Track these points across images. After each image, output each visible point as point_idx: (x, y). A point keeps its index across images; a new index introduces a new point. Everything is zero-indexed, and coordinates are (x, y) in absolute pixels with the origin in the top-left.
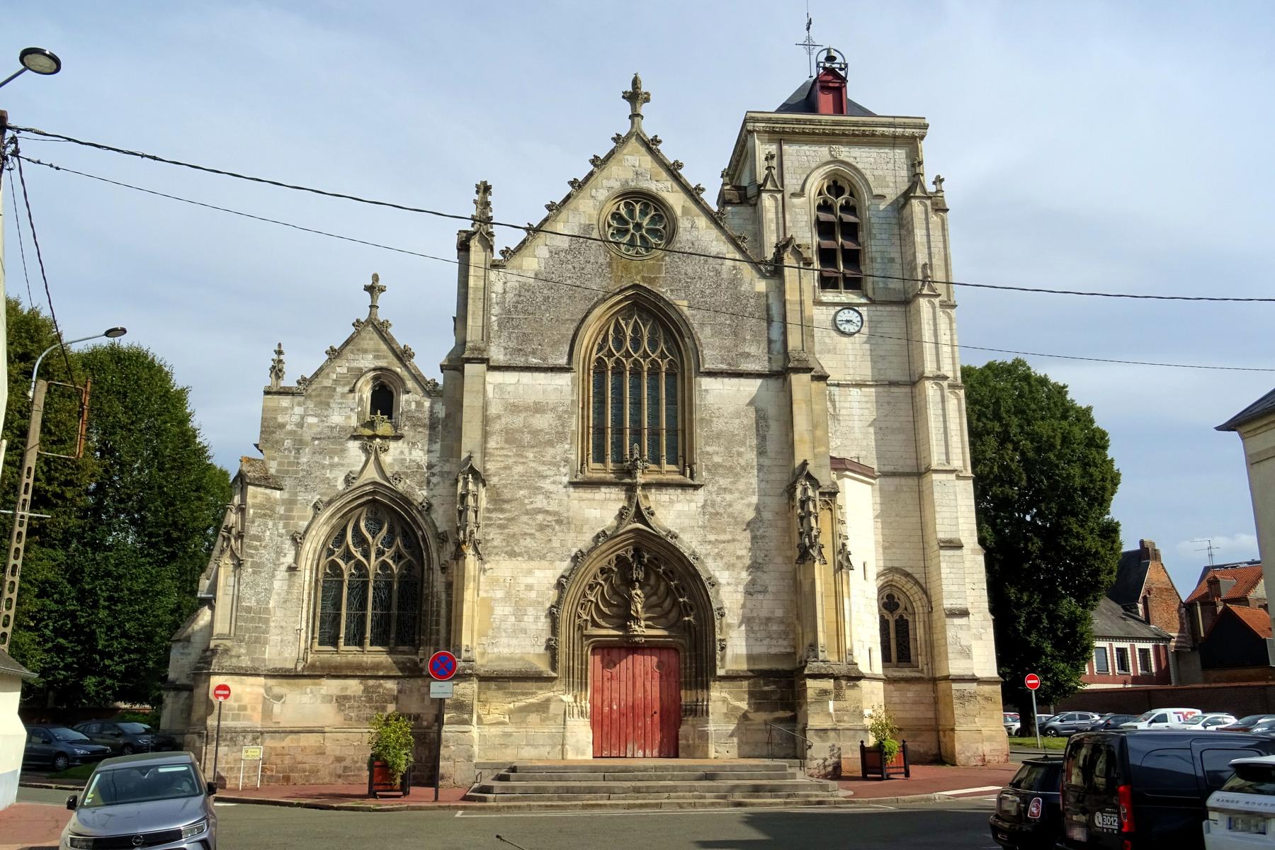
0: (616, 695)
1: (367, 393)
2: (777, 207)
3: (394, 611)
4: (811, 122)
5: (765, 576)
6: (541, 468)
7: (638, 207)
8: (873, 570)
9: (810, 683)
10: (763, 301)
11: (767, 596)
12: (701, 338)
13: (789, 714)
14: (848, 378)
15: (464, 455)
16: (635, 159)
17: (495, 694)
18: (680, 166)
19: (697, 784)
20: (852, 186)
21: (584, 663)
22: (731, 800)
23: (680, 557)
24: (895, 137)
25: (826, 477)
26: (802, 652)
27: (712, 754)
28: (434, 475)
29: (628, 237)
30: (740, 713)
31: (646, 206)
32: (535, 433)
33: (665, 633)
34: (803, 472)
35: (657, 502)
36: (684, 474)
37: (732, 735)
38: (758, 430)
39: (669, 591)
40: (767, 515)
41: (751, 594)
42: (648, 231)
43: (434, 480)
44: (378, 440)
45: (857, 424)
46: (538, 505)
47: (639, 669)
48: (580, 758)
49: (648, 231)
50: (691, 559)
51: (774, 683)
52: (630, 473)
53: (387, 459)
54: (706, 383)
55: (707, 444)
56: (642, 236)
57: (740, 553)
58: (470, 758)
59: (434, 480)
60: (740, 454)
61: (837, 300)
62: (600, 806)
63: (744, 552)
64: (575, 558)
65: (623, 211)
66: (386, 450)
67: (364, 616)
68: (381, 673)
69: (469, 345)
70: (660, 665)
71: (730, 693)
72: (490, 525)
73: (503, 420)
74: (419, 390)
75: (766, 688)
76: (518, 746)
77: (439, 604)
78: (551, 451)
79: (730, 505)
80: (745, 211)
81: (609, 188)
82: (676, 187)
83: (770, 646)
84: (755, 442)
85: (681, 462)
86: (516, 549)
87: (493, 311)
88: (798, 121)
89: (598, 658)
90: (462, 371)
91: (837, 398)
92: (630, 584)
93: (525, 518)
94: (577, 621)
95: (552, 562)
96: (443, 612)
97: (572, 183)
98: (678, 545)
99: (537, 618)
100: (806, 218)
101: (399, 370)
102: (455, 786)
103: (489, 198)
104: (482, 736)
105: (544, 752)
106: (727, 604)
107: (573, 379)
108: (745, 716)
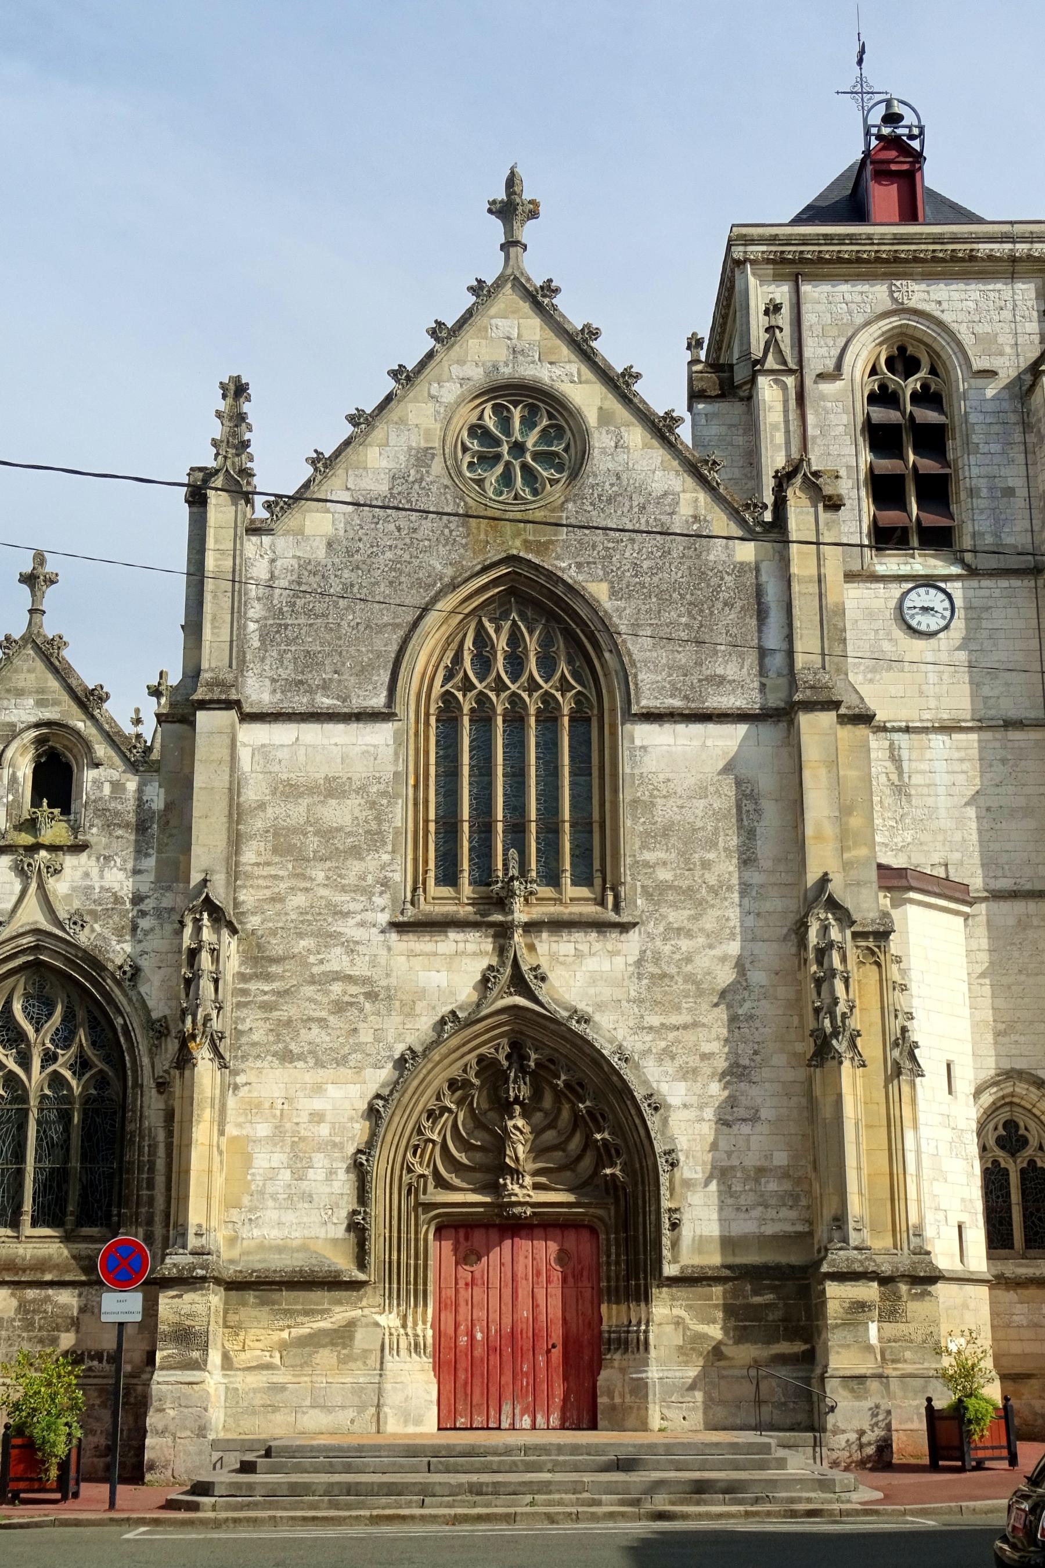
0: (480, 1314)
1: (25, 769)
2: (786, 402)
3: (75, 1163)
4: (852, 239)
5: (754, 1091)
6: (339, 898)
7: (517, 413)
8: (966, 1079)
9: (832, 1289)
10: (750, 579)
11: (762, 1128)
12: (634, 650)
13: (799, 1347)
14: (927, 716)
15: (196, 878)
16: (513, 324)
17: (254, 1312)
18: (595, 334)
19: (587, 1478)
20: (934, 355)
21: (421, 1255)
22: (648, 1507)
23: (597, 1059)
24: (1013, 260)
25: (867, 903)
26: (821, 1232)
27: (655, 1421)
28: (143, 914)
29: (499, 469)
30: (708, 1347)
31: (533, 410)
32: (327, 834)
33: (570, 1198)
34: (822, 897)
35: (553, 957)
36: (602, 903)
37: (692, 1387)
38: (740, 820)
39: (577, 1119)
40: (758, 977)
41: (727, 1124)
42: (536, 456)
43: (144, 923)
44: (43, 853)
45: (943, 802)
47: (524, 1264)
48: (411, 1429)
49: (536, 456)
50: (614, 1060)
51: (773, 1289)
52: (502, 903)
53: (59, 887)
54: (643, 734)
55: (644, 846)
56: (524, 467)
57: (706, 1048)
58: (202, 1431)
59: (144, 923)
60: (706, 865)
61: (905, 570)
62: (403, 1518)
63: (715, 1047)
64: (401, 1063)
65: (490, 422)
66: (57, 872)
67: (20, 1173)
68: (48, 1277)
69: (206, 676)
70: (563, 1257)
71: (689, 1308)
72: (245, 1005)
74: (117, 760)
75: (757, 1300)
76: (297, 1409)
78: (355, 867)
79: (689, 960)
80: (730, 410)
81: (463, 381)
82: (587, 373)
83: (762, 1221)
84: (734, 841)
85: (598, 882)
86: (293, 1046)
87: (251, 613)
88: (829, 239)
89: (448, 1245)
90: (192, 724)
91: (905, 754)
92: (505, 1108)
93: (309, 990)
94: (406, 1178)
95: (359, 1069)
96: (160, 1164)
97: (395, 374)
98: (591, 1035)
99: (331, 1173)
100: (845, 419)
101: (80, 725)
102: (175, 1482)
103: (246, 407)
104: (225, 1389)
105: (343, 1418)
106: (682, 1143)
107: (396, 733)
108: (717, 1352)
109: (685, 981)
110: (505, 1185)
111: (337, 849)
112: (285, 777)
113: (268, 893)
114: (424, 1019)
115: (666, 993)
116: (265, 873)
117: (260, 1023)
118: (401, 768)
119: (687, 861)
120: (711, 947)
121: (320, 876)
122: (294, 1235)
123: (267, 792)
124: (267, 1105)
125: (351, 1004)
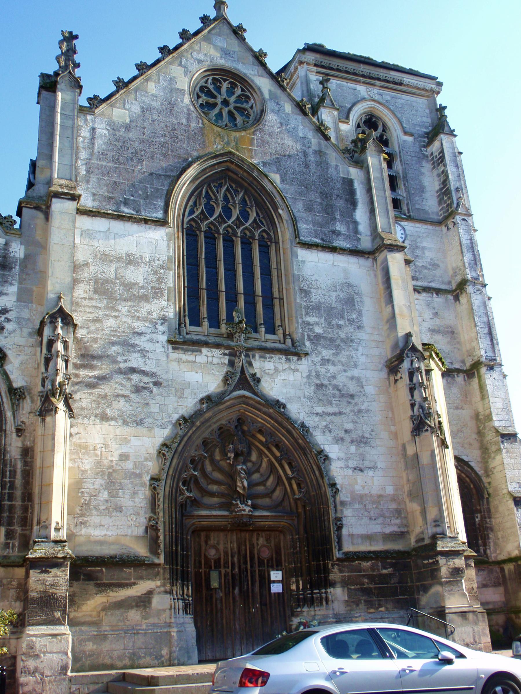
5: (373, 452)
7: (225, 86)
11: (380, 473)
31: (233, 86)
32: (129, 286)
46: (134, 365)
54: (302, 254)
55: (307, 314)
73: (92, 269)
75: (385, 571)
77: (13, 473)
79: (334, 377)
86: (108, 411)
93: (119, 378)
95: (150, 429)
109: (333, 389)
110: (237, 504)
111: (134, 295)
112: (102, 250)
113: (91, 316)
114: (190, 400)
116: (89, 304)
117: (86, 396)
118: (171, 254)
119: (329, 324)
120: (345, 371)
121: (124, 310)
122: (109, 533)
124: (92, 448)
125: (145, 388)
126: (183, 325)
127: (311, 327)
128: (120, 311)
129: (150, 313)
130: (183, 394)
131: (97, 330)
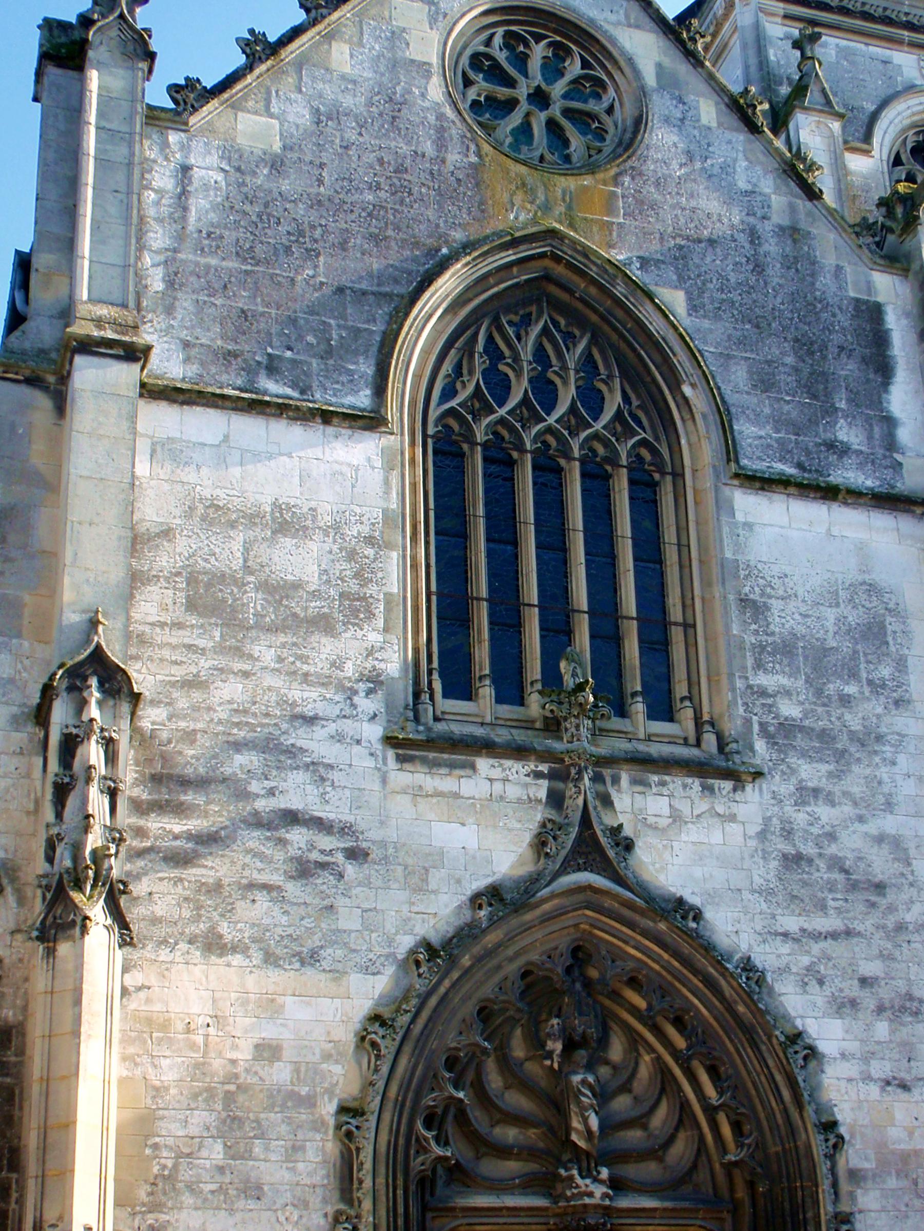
32: (279, 591)
46: (293, 802)
54: (747, 504)
55: (759, 665)
73: (182, 545)
79: (832, 837)
86: (224, 928)
93: (253, 839)
95: (338, 974)
109: (830, 868)
110: (571, 1178)
111: (295, 615)
112: (207, 493)
113: (178, 672)
114: (444, 898)
115: (805, 884)
116: (174, 641)
117: (164, 886)
118: (394, 505)
119: (819, 692)
120: (861, 819)
123: (178, 512)
124: (180, 1026)
125: (323, 866)
126: (425, 697)
127: (770, 701)
128: (257, 659)
129: (337, 665)
130: (426, 881)
131: (196, 708)
